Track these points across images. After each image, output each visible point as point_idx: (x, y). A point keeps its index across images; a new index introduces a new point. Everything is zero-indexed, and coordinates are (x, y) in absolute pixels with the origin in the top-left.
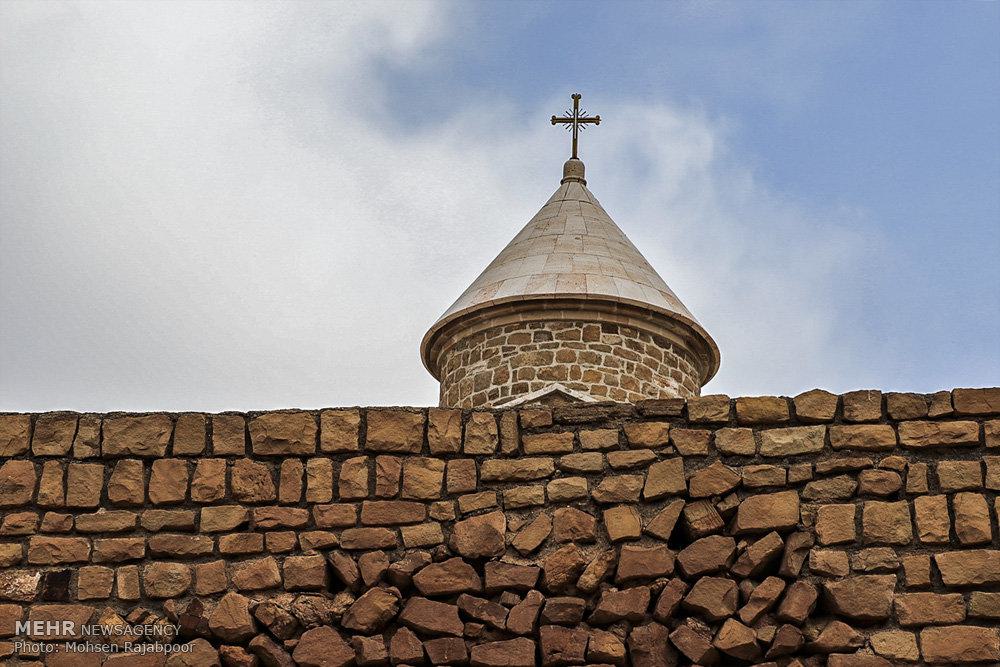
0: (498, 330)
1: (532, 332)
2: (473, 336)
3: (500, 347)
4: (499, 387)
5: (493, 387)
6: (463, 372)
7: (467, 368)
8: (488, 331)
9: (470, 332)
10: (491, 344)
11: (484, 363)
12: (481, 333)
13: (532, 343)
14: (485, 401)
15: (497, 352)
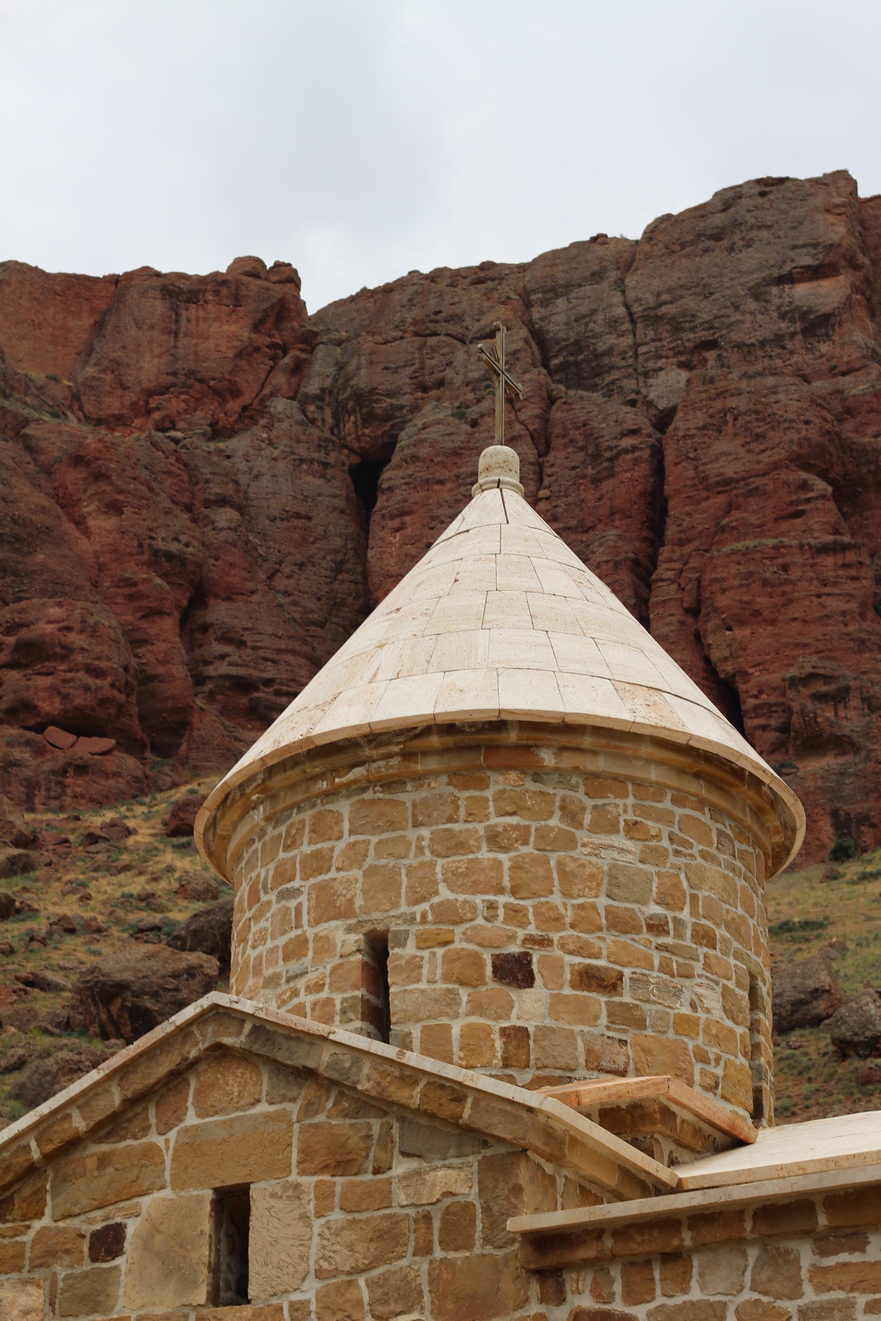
0: (659, 791)
1: (715, 826)
2: (596, 776)
3: (665, 831)
4: (670, 915)
5: (655, 909)
6: (570, 843)
7: (582, 836)
8: (639, 784)
9: (599, 764)
10: (647, 813)
11: (629, 844)
12: (618, 779)
13: (713, 850)
14: (637, 929)
15: (658, 837)
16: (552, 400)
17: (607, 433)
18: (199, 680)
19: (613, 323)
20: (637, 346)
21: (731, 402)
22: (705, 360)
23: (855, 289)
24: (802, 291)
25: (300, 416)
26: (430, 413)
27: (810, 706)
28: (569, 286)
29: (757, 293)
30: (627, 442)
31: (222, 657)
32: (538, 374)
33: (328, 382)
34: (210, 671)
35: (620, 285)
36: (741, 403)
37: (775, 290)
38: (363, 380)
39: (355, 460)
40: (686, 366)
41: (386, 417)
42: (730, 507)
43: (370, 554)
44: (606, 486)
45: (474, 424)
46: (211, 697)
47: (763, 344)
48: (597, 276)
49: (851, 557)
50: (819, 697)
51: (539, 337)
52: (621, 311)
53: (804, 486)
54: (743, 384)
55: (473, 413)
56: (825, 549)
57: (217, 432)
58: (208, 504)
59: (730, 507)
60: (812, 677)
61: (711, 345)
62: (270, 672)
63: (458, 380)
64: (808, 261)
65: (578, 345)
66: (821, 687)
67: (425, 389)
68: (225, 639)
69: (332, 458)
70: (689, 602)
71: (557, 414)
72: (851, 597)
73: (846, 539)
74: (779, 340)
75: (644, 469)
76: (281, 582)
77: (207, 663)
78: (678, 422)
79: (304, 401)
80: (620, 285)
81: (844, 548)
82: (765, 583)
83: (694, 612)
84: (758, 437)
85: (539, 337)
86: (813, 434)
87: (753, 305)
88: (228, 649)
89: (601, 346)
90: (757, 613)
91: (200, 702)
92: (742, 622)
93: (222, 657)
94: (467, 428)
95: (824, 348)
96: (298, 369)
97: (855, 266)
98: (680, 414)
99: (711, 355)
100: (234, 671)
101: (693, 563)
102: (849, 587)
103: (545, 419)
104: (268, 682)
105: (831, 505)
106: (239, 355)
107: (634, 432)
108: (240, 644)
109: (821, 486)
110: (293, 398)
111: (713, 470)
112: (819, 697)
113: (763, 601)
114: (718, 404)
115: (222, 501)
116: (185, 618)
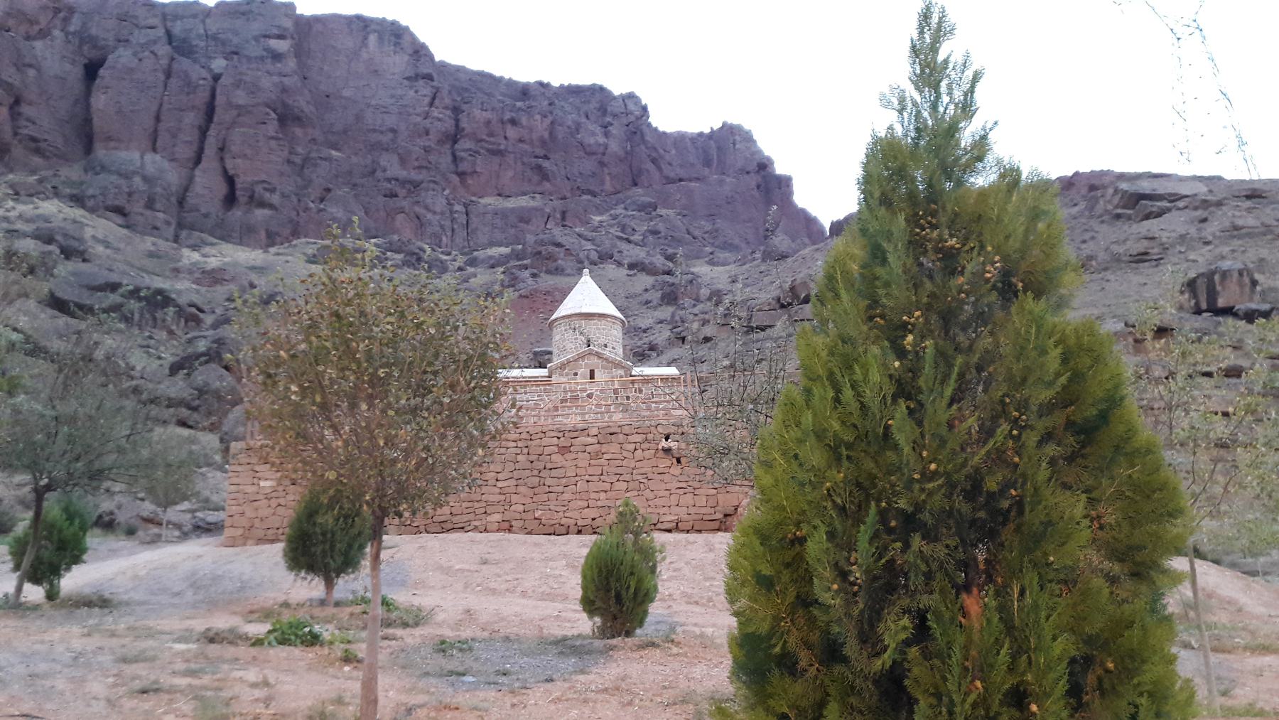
16: (173, 59)
17: (194, 76)
18: (16, 134)
19: (199, 36)
20: (207, 47)
21: (244, 77)
22: (232, 59)
23: (292, 46)
24: (274, 43)
25: (64, 38)
26: (121, 51)
27: (262, 191)
28: (182, 18)
29: (256, 39)
30: (201, 82)
31: (27, 127)
32: (168, 48)
33: (78, 29)
34: (20, 131)
35: (203, 22)
36: (247, 79)
37: (262, 40)
38: (94, 31)
39: (87, 61)
40: (226, 59)
41: (103, 48)
42: (239, 115)
43: (92, 100)
44: (191, 96)
45: (140, 60)
46: (20, 141)
47: (256, 58)
48: (195, 16)
49: (282, 143)
50: (266, 189)
51: (169, 35)
52: (202, 31)
53: (268, 114)
54: (249, 72)
55: (141, 55)
56: (272, 138)
57: (28, 38)
58: (25, 65)
59: (239, 115)
60: (264, 181)
61: (236, 53)
62: (46, 137)
63: (134, 42)
64: (277, 32)
65: (184, 41)
66: (266, 186)
67: (120, 41)
68: (28, 120)
69: (77, 59)
70: (220, 145)
71: (175, 66)
72: (280, 156)
73: (281, 136)
74: (262, 58)
75: (207, 94)
76: (51, 102)
77: (19, 128)
78: (222, 81)
79: (67, 34)
80: (203, 22)
81: (280, 139)
82: (250, 145)
83: (222, 149)
84: (253, 93)
85: (169, 35)
86: (274, 97)
87: (254, 43)
88: (28, 124)
89: (194, 43)
90: (245, 155)
91: (15, 142)
92: (239, 157)
93: (27, 127)
94: (136, 61)
95: (279, 65)
96: (66, 20)
97: (293, 38)
98: (223, 77)
99: (235, 57)
100: (31, 133)
101: (224, 132)
102: (280, 153)
103: (170, 66)
104: (46, 140)
105: (276, 122)
106: (41, 8)
107: (204, 79)
108: (34, 123)
109: (273, 115)
110: (62, 30)
111: (234, 100)
112: (266, 189)
113: (248, 152)
114: (238, 77)
115: (30, 66)
116: (11, 108)
